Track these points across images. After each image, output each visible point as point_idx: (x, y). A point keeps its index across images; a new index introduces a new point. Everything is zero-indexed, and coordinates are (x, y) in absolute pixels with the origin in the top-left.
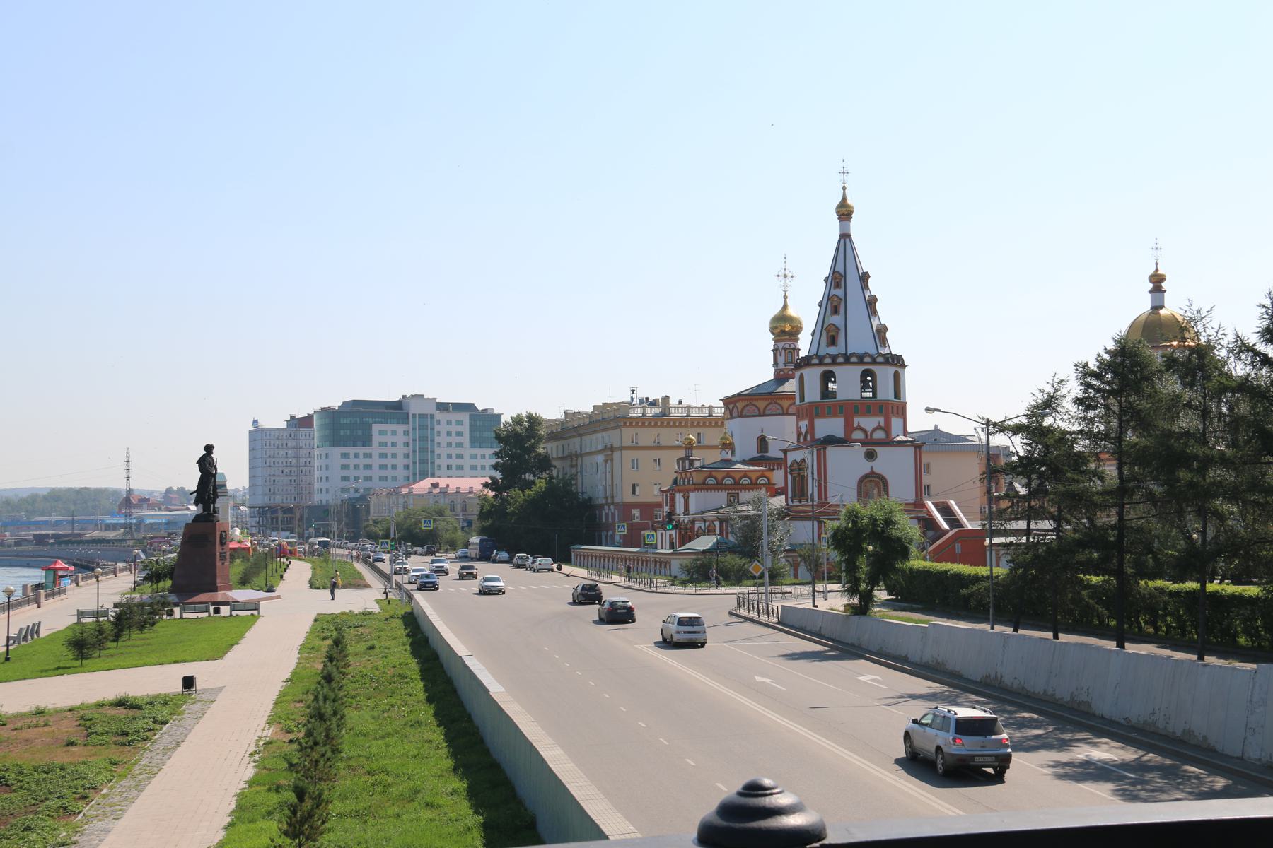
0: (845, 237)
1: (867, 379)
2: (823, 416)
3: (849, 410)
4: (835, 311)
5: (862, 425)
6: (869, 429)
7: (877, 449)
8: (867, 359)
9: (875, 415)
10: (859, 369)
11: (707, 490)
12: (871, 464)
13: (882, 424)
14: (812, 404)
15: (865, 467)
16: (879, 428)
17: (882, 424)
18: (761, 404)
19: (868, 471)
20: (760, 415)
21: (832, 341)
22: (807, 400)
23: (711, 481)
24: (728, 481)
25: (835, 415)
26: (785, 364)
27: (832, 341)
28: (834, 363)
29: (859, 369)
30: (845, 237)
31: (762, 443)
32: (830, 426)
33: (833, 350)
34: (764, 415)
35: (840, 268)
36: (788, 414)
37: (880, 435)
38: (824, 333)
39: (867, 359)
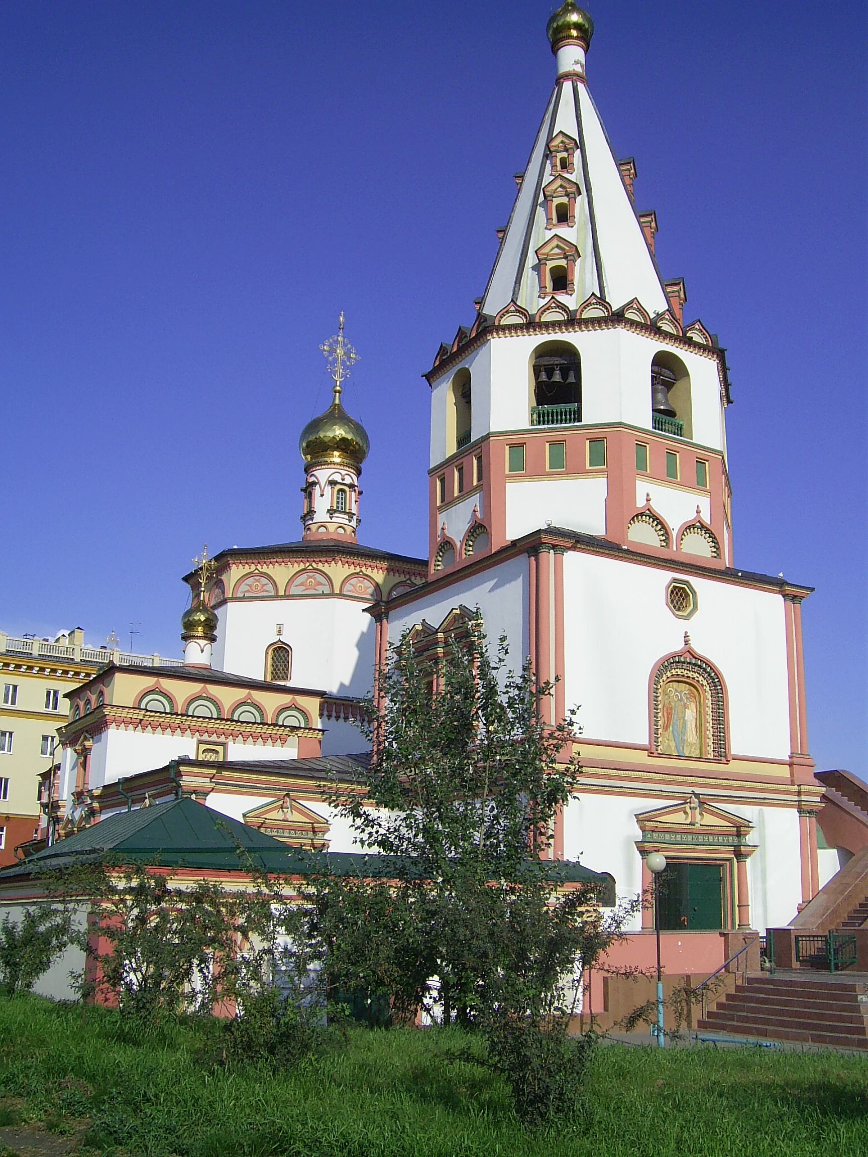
1: (667, 373)
2: (538, 474)
6: (674, 524)
7: (697, 583)
11: (139, 724)
12: (683, 626)
13: (706, 518)
15: (666, 635)
18: (281, 572)
19: (678, 646)
20: (276, 597)
21: (561, 281)
23: (156, 703)
24: (202, 709)
25: (578, 471)
26: (331, 512)
31: (281, 654)
34: (287, 597)
36: (341, 595)
37: (697, 547)
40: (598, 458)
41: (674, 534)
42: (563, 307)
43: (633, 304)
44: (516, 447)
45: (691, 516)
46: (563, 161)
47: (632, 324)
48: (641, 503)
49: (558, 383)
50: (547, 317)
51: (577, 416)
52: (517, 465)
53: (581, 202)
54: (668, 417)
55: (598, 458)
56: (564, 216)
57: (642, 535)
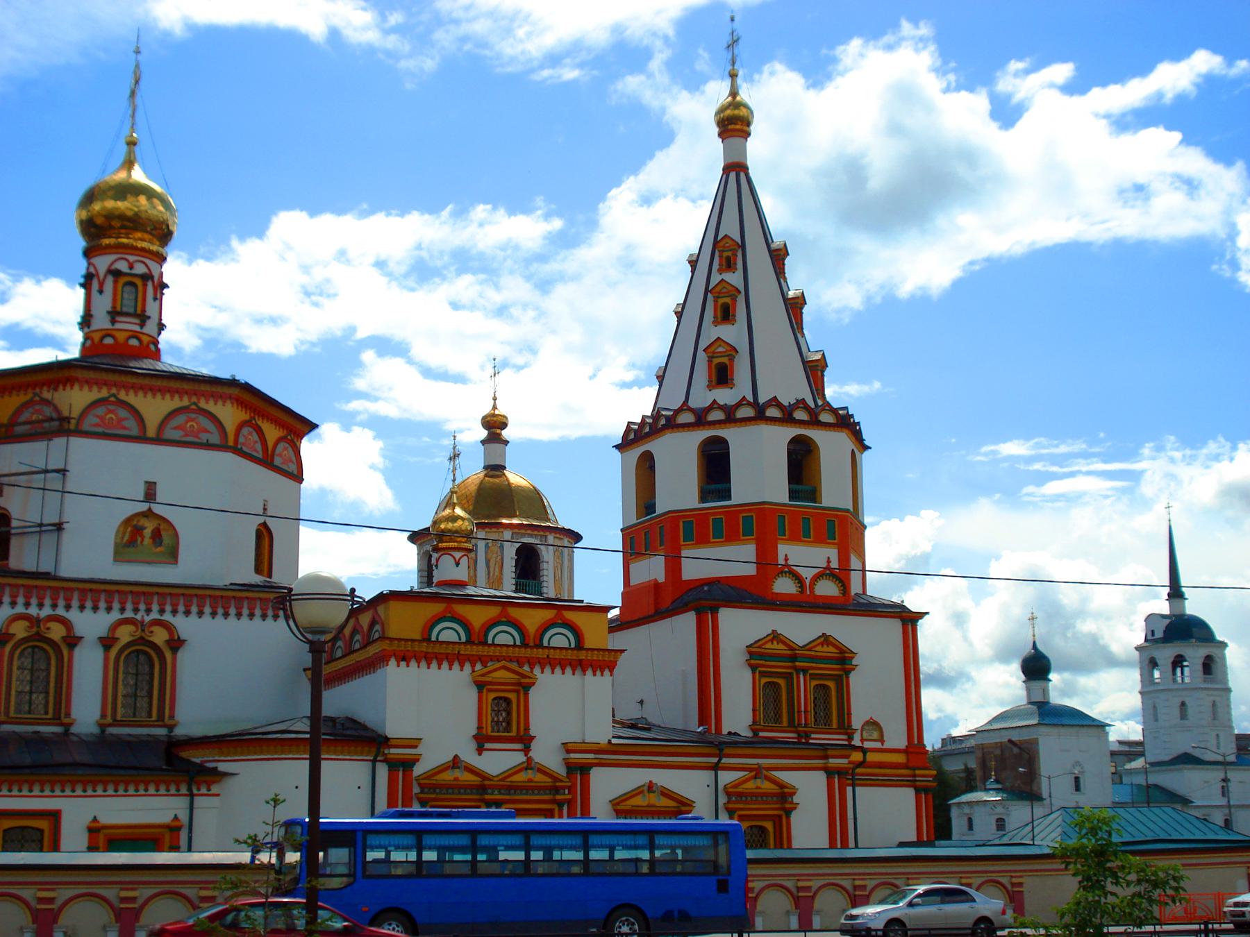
0: (736, 169)
2: (702, 540)
3: (761, 525)
4: (726, 315)
6: (807, 574)
8: (800, 415)
9: (820, 540)
10: (788, 433)
13: (835, 564)
14: (674, 517)
16: (826, 573)
17: (834, 564)
21: (722, 376)
22: (660, 508)
27: (722, 376)
29: (788, 433)
30: (736, 169)
32: (733, 560)
33: (725, 396)
35: (730, 228)
37: (827, 589)
38: (702, 357)
39: (800, 415)
41: (808, 582)
42: (721, 407)
46: (728, 259)
47: (773, 420)
48: (781, 561)
49: (715, 465)
53: (741, 300)
57: (784, 586)
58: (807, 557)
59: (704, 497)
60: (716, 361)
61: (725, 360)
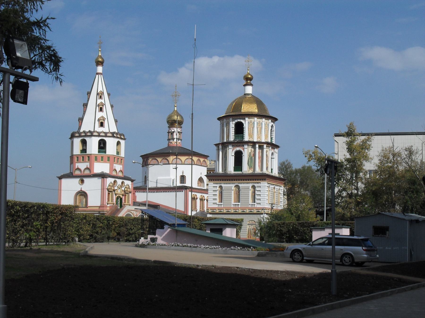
2: (99, 162)
5: (116, 169)
16: (121, 171)
21: (102, 125)
22: (88, 152)
25: (105, 162)
27: (102, 125)
28: (106, 136)
29: (117, 140)
37: (120, 174)
39: (118, 136)
40: (109, 160)
43: (114, 133)
44: (96, 157)
45: (120, 169)
46: (101, 96)
49: (102, 145)
50: (102, 134)
51: (105, 152)
52: (96, 159)
54: (118, 153)
55: (109, 160)
56: (101, 110)
57: (114, 173)
58: (118, 167)
59: (99, 152)
60: (101, 121)
61: (103, 121)
